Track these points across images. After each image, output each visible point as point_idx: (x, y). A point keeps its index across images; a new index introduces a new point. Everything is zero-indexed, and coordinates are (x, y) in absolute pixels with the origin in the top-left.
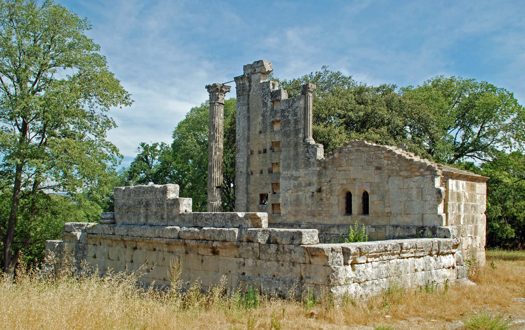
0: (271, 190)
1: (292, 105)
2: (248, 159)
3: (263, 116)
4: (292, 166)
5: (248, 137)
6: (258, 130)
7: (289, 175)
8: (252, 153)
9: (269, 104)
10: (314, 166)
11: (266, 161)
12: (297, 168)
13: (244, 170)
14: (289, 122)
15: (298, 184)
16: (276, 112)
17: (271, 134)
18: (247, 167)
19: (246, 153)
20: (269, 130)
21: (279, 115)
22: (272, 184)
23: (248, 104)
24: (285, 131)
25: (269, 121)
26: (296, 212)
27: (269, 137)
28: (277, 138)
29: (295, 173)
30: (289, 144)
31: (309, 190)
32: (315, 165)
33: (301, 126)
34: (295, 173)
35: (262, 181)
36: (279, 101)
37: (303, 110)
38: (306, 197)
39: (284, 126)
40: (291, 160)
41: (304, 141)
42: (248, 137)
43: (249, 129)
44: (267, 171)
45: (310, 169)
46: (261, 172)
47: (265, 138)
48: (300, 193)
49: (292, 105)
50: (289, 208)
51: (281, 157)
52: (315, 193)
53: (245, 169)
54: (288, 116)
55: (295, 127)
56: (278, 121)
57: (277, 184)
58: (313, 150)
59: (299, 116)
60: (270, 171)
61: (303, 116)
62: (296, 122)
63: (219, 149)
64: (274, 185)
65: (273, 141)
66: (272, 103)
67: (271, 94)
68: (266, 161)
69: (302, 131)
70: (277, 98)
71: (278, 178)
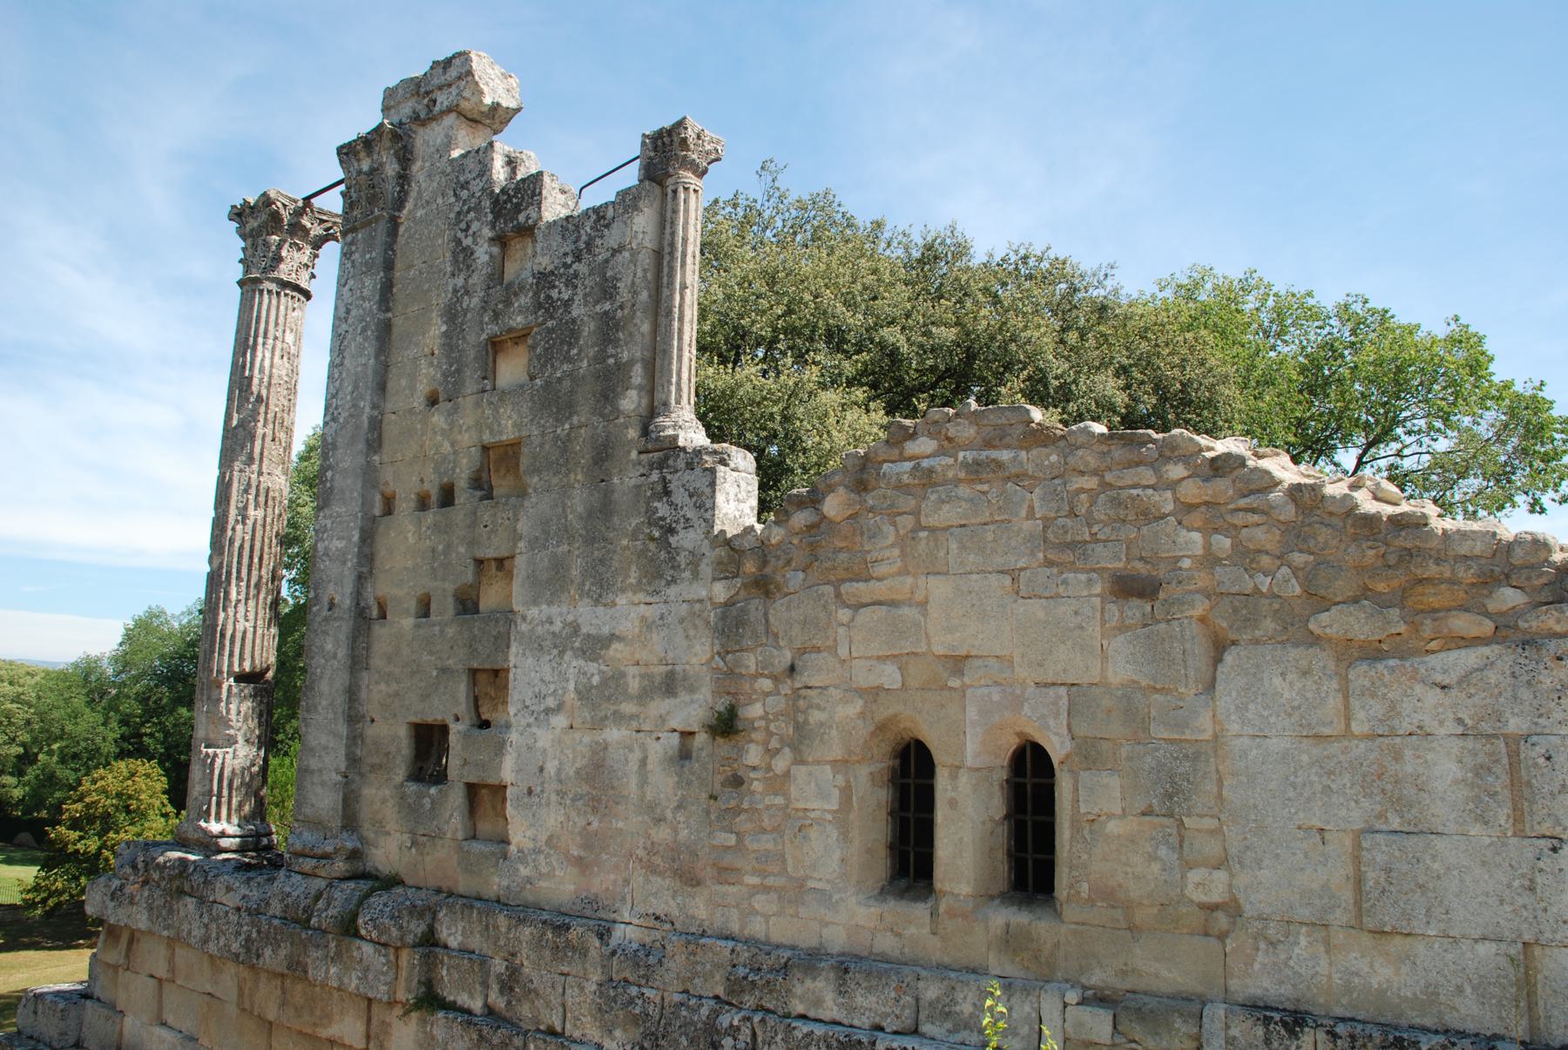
0: (462, 706)
3: (452, 315)
4: (575, 573)
5: (376, 425)
6: (423, 388)
10: (696, 575)
12: (601, 587)
15: (605, 682)
17: (478, 405)
18: (361, 579)
19: (355, 506)
20: (471, 386)
22: (473, 673)
23: (389, 266)
24: (548, 384)
25: (474, 338)
27: (470, 421)
29: (590, 617)
30: (564, 450)
32: (706, 569)
34: (590, 617)
35: (426, 657)
40: (571, 539)
41: (645, 432)
42: (376, 425)
43: (382, 387)
44: (451, 600)
45: (672, 591)
46: (424, 609)
47: (452, 424)
51: (523, 526)
52: (701, 738)
53: (349, 588)
56: (520, 337)
57: (496, 673)
60: (467, 604)
64: (482, 677)
65: (487, 438)
71: (502, 642)
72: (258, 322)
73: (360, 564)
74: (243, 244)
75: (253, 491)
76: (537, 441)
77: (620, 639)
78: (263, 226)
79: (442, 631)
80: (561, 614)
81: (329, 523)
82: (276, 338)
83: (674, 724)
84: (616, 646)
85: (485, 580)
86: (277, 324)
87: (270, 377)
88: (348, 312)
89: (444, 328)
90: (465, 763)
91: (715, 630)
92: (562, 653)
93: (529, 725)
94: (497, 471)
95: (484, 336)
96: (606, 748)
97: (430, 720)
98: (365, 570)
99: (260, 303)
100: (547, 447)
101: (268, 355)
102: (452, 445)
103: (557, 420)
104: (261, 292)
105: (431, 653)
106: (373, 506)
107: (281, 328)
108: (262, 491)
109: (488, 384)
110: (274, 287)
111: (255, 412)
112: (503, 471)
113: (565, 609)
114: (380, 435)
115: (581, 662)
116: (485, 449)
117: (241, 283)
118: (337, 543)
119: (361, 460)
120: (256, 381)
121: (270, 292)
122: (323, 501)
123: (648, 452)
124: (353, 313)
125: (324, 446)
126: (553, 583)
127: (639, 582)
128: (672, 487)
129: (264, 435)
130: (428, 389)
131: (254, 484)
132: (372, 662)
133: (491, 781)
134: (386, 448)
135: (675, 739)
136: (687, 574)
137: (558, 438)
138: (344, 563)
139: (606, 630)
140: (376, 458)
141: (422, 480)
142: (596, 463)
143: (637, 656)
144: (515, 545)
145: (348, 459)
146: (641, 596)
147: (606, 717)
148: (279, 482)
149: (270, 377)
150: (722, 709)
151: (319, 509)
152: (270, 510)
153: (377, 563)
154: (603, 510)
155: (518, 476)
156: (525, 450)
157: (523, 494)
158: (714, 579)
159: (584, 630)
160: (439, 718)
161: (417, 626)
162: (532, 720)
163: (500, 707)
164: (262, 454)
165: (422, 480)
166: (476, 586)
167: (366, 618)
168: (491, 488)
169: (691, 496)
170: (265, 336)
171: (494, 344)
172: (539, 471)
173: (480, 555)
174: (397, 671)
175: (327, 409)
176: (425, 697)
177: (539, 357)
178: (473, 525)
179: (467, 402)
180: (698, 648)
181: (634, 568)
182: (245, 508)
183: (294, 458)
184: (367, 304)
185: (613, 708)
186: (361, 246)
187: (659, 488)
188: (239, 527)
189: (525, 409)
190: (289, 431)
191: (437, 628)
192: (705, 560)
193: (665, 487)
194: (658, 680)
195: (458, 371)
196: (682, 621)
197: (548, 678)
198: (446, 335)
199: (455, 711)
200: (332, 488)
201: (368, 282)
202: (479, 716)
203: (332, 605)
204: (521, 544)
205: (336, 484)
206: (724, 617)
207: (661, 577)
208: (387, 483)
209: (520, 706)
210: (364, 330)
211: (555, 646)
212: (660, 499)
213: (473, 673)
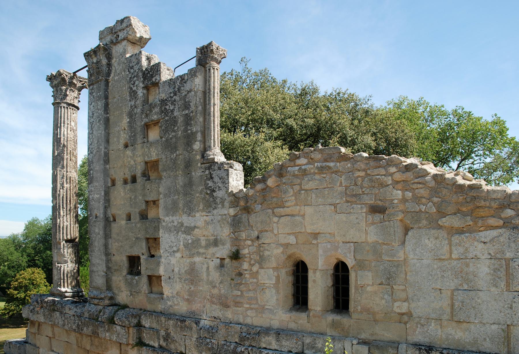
0: (144, 250)
1: (179, 89)
2: (107, 194)
3: (131, 115)
4: (181, 205)
5: (107, 155)
6: (122, 141)
7: (176, 224)
8: (114, 183)
9: (140, 93)
10: (223, 206)
11: (136, 196)
12: (190, 210)
14: (174, 121)
15: (193, 242)
16: (152, 107)
17: (142, 147)
18: (106, 208)
19: (102, 183)
20: (139, 141)
21: (157, 110)
22: (147, 239)
23: (106, 98)
24: (167, 140)
25: (139, 124)
27: (140, 153)
28: (154, 154)
29: (187, 220)
30: (174, 163)
31: (214, 254)
32: (227, 204)
33: (196, 128)
34: (187, 220)
35: (131, 234)
36: (156, 84)
37: (200, 95)
38: (208, 268)
39: (166, 131)
40: (179, 194)
41: (203, 157)
42: (107, 155)
43: (108, 141)
44: (138, 215)
45: (215, 212)
47: (134, 154)
48: (197, 259)
49: (179, 89)
50: (178, 287)
51: (161, 190)
52: (227, 260)
53: (102, 211)
54: (172, 111)
55: (186, 130)
56: (156, 123)
57: (155, 239)
58: (222, 174)
59: (193, 108)
60: (144, 216)
61: (200, 108)
62: (188, 120)
63: (70, 180)
64: (150, 241)
65: (147, 159)
66: (145, 91)
67: (144, 73)
69: (199, 137)
70: (154, 79)
71: (157, 229)
72: (61, 118)
73: (105, 203)
74: (53, 90)
75: (65, 178)
76: (164, 160)
77: (198, 228)
78: (59, 83)
79: (135, 225)
80: (177, 219)
81: (93, 189)
82: (68, 124)
83: (218, 256)
84: (196, 230)
85: (149, 208)
86: (68, 119)
87: (67, 138)
88: (93, 114)
89: (128, 120)
90: (147, 269)
91: (231, 225)
92: (178, 233)
93: (168, 256)
94: (151, 170)
95: (143, 123)
96: (195, 264)
97: (134, 254)
98: (107, 205)
99: (61, 111)
100: (168, 162)
101: (66, 130)
102: (134, 162)
103: (171, 153)
104: (61, 107)
105: (132, 233)
106: (108, 183)
107: (69, 120)
108: (68, 178)
109: (146, 140)
110: (65, 105)
111: (63, 151)
112: (153, 171)
113: (178, 218)
114: (108, 158)
115: (185, 236)
116: (146, 163)
117: (53, 104)
118: (97, 195)
119: (102, 167)
120: (62, 139)
121: (64, 107)
122: (90, 181)
124: (95, 115)
125: (89, 162)
126: (173, 209)
127: (203, 208)
128: (213, 176)
129: (67, 158)
130: (124, 142)
131: (65, 175)
132: (112, 236)
133: (156, 274)
134: (111, 162)
135: (218, 261)
136: (220, 206)
137: (172, 159)
138: (99, 202)
139: (193, 225)
141: (124, 174)
142: (186, 168)
143: (204, 234)
144: (159, 196)
145: (98, 167)
146: (204, 213)
147: (194, 254)
148: (74, 175)
149: (67, 138)
150: (234, 251)
151: (89, 184)
152: (72, 184)
153: (111, 202)
154: (190, 184)
155: (158, 172)
156: (160, 163)
157: (160, 178)
158: (230, 207)
159: (185, 225)
160: (137, 254)
161: (127, 224)
162: (169, 255)
163: (157, 250)
164: (67, 165)
165: (124, 174)
166: (146, 210)
167: (109, 221)
168: (149, 176)
169: (220, 179)
170: (64, 123)
171: (147, 126)
172: (165, 170)
173: (147, 199)
174: (121, 238)
175: (88, 149)
176: (131, 247)
177: (163, 130)
178: (144, 189)
179: (139, 146)
180: (225, 231)
181: (201, 204)
182: (63, 184)
183: (78, 166)
184: (100, 112)
185: (197, 251)
186: (96, 90)
187: (209, 176)
188: (61, 190)
189: (159, 149)
190: (76, 157)
191: (134, 224)
192: (226, 201)
193: (211, 176)
194: (212, 241)
195: (134, 135)
196: (219, 221)
197: (173, 241)
198: (129, 122)
199: (142, 252)
202: (150, 253)
203: (96, 217)
204: (161, 196)
205: (94, 175)
206: (233, 220)
207: (211, 207)
208: (112, 175)
209: (164, 250)
210: (99, 121)
211: (175, 230)
212: (209, 180)
213: (147, 239)
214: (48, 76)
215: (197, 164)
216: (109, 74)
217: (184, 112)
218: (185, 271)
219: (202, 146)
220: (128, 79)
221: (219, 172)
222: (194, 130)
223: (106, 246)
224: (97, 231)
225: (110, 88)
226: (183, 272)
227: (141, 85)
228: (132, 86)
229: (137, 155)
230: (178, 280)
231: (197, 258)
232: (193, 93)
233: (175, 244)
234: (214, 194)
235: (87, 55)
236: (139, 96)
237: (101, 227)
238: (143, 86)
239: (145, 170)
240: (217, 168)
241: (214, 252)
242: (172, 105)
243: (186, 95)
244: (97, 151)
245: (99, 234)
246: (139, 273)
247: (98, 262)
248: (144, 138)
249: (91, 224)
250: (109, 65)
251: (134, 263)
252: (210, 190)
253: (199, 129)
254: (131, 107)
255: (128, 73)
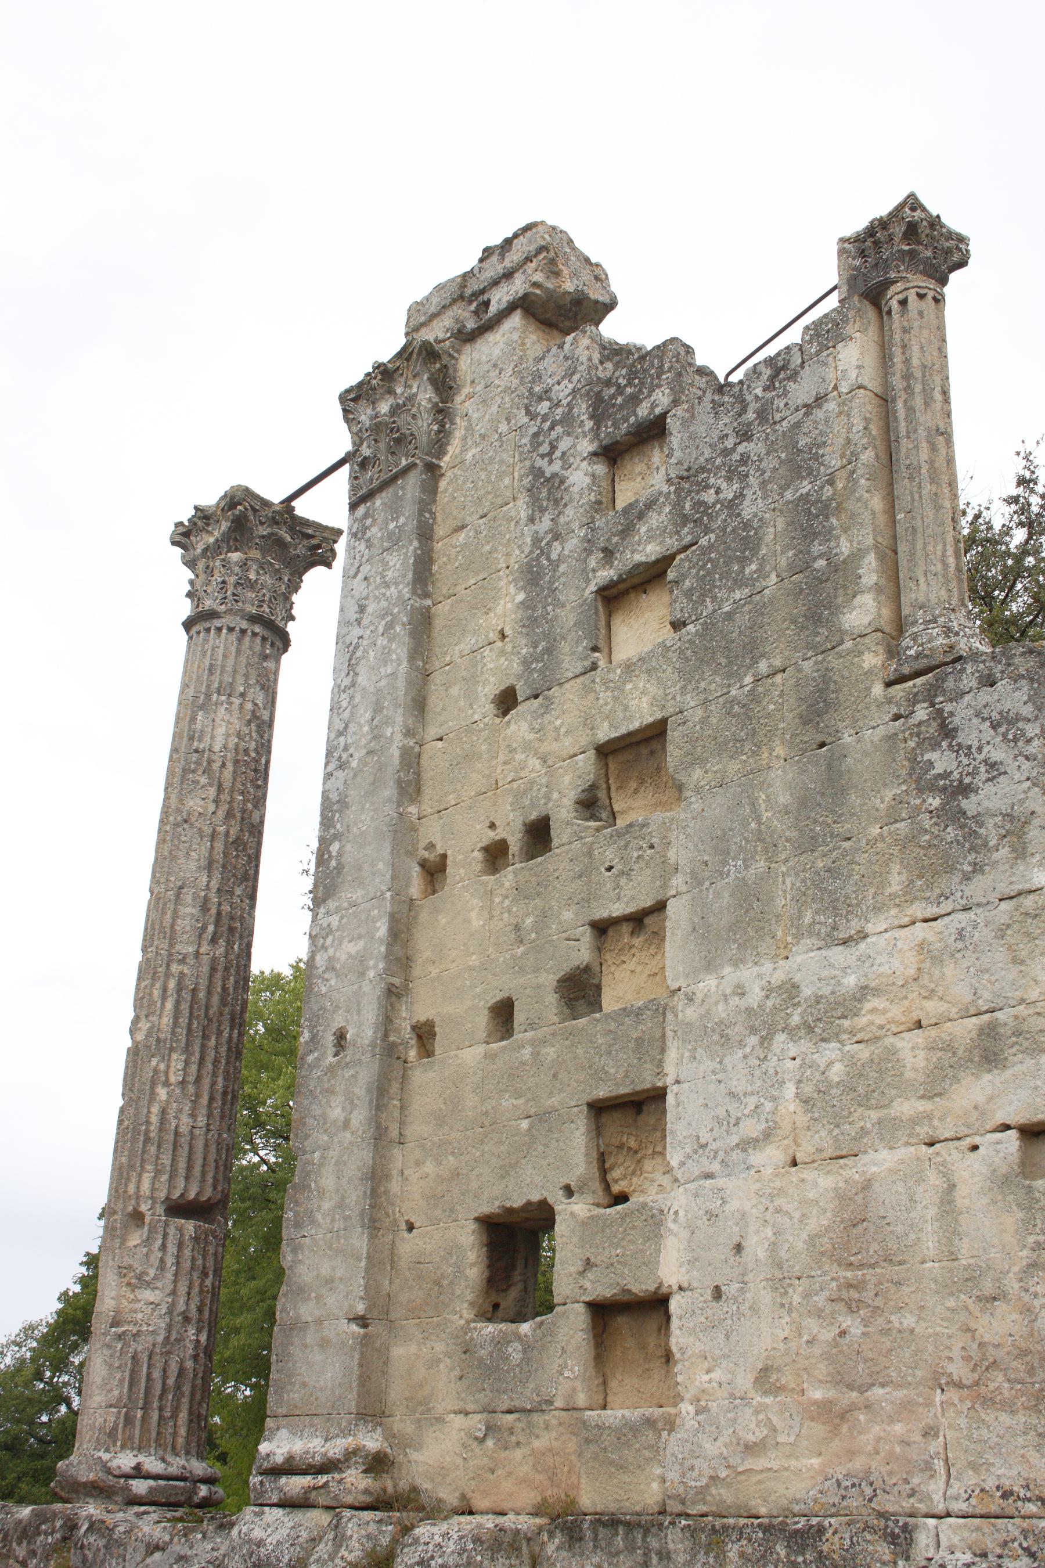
2: (401, 933)
3: (535, 576)
5: (411, 761)
6: (490, 688)
7: (755, 996)
8: (434, 871)
11: (544, 915)
12: (836, 916)
13: (363, 1029)
23: (425, 534)
26: (841, 1380)
35: (508, 1102)
37: (863, 406)
40: (770, 849)
42: (411, 761)
43: (419, 705)
45: (977, 888)
48: (881, 1160)
49: (762, 415)
50: (766, 1334)
54: (732, 506)
55: (802, 565)
61: (867, 456)
62: (812, 519)
66: (600, 468)
68: (544, 915)
69: (870, 571)
79: (536, 1055)
81: (334, 921)
88: (362, 609)
89: (521, 597)
92: (766, 1040)
98: (396, 981)
106: (408, 885)
114: (418, 774)
119: (390, 810)
123: (901, 679)
124: (370, 610)
132: (408, 1132)
134: (427, 791)
136: (1004, 852)
140: (413, 809)
144: (665, 886)
146: (919, 910)
153: (417, 971)
159: (807, 992)
165: (492, 826)
169: (994, 727)
181: (895, 867)
187: (933, 729)
189: (670, 673)
193: (943, 725)
195: (548, 651)
196: (1001, 932)
200: (340, 867)
201: (395, 560)
205: (347, 859)
207: (951, 869)
210: (389, 626)
211: (753, 1030)
212: (935, 746)
214: (179, 524)
215: (868, 689)
216: (440, 443)
217: (788, 495)
218: (812, 1240)
219: (886, 612)
220: (525, 440)
221: (985, 696)
222: (845, 548)
223: (376, 1179)
224: (336, 1113)
225: (442, 498)
226: (800, 1246)
227: (586, 446)
228: (540, 463)
229: (557, 730)
230: (766, 1297)
231: (884, 1154)
232: (831, 406)
233: (752, 1101)
234: (965, 804)
235: (353, 399)
236: (575, 489)
237: (360, 1090)
238: (592, 448)
239: (593, 787)
240: (974, 684)
241: (981, 1099)
242: (729, 480)
243: (798, 425)
244: (370, 752)
245: (346, 1124)
246: (538, 1303)
247: (325, 1270)
248: (595, 649)
249: (312, 1084)
250: (443, 413)
251: (515, 1243)
252: (944, 790)
253: (870, 541)
254: (536, 540)
255: (526, 420)
